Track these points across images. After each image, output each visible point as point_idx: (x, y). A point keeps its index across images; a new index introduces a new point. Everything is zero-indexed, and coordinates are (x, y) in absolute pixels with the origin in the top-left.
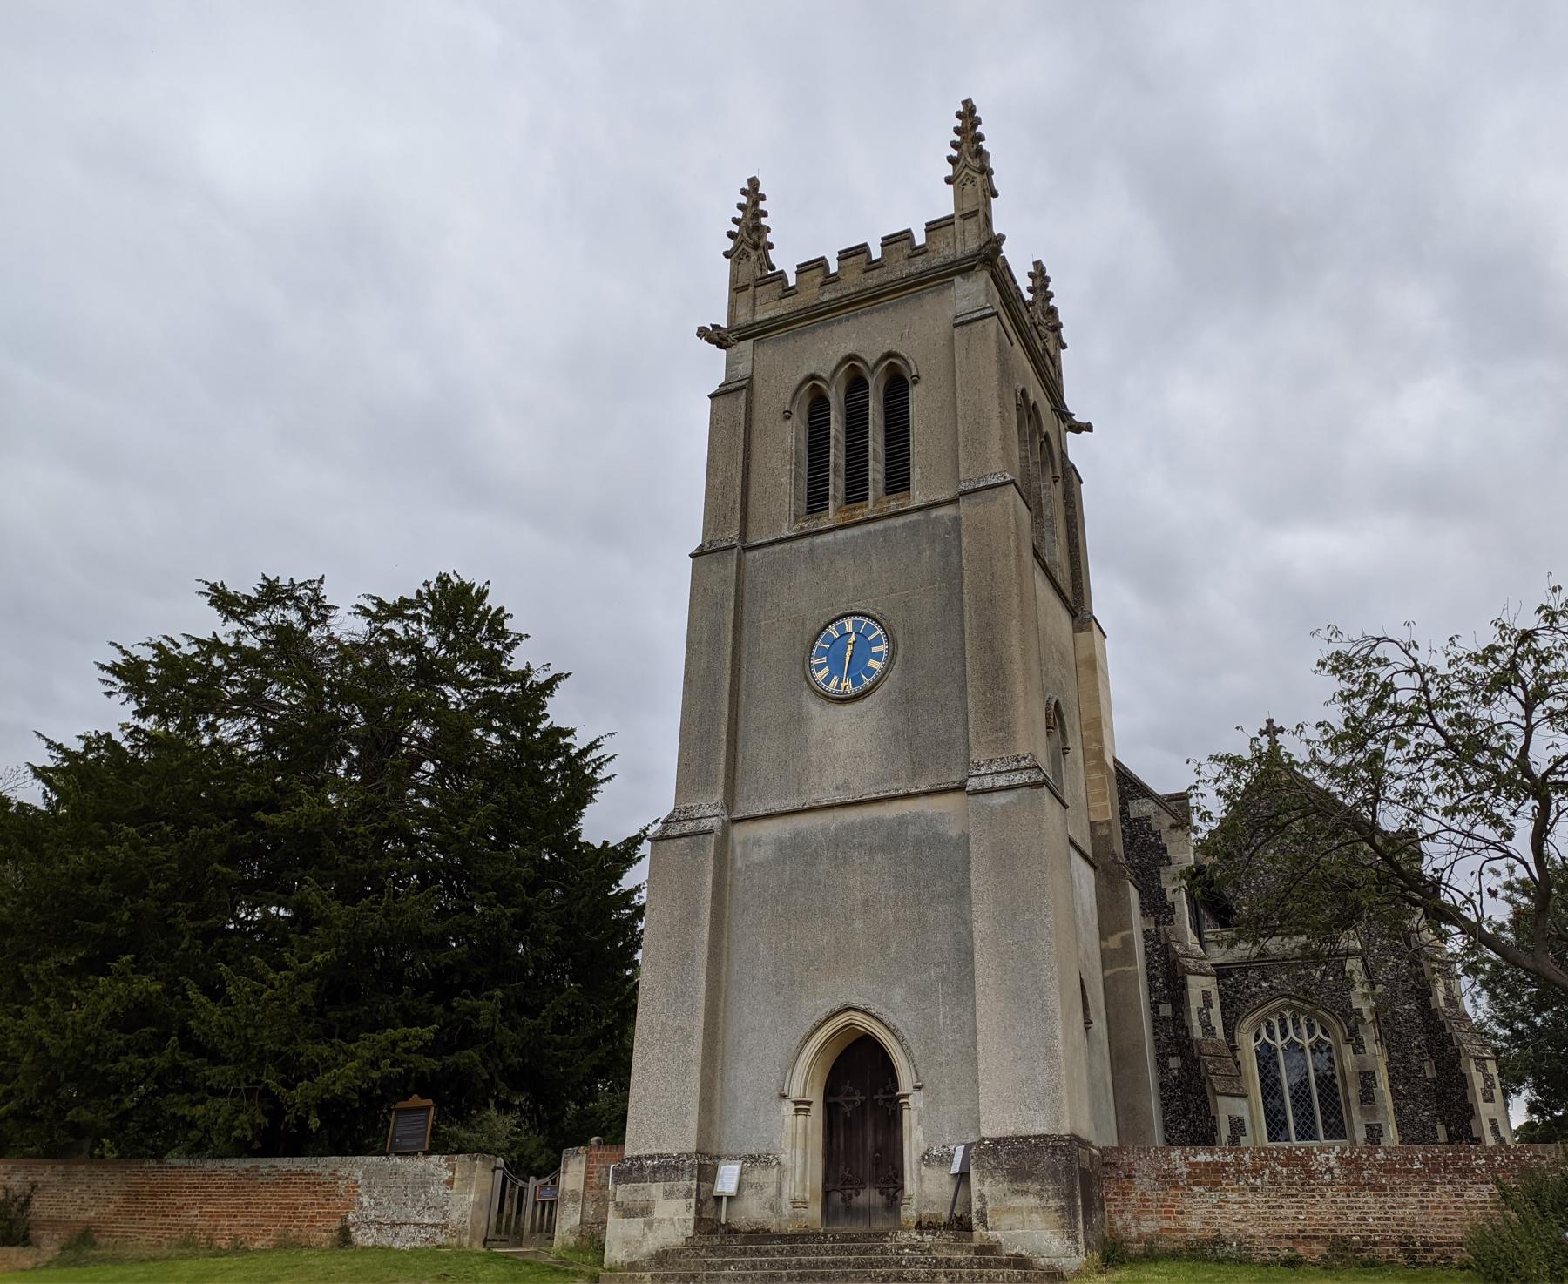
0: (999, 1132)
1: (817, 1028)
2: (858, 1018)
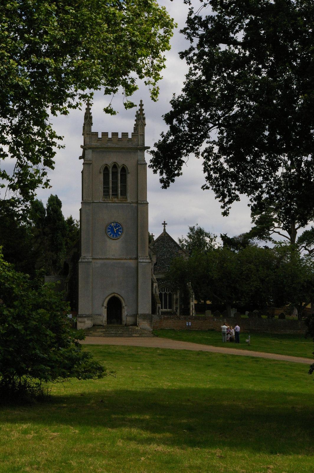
0: (141, 313)
1: (109, 296)
2: (116, 295)
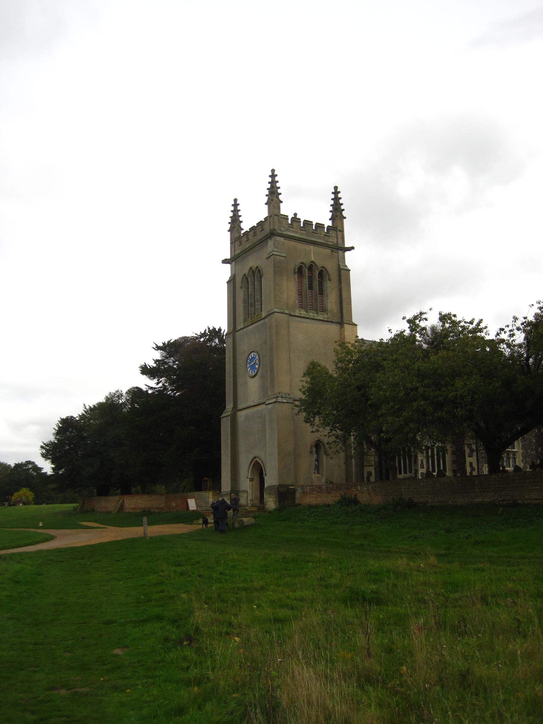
2: (258, 460)
